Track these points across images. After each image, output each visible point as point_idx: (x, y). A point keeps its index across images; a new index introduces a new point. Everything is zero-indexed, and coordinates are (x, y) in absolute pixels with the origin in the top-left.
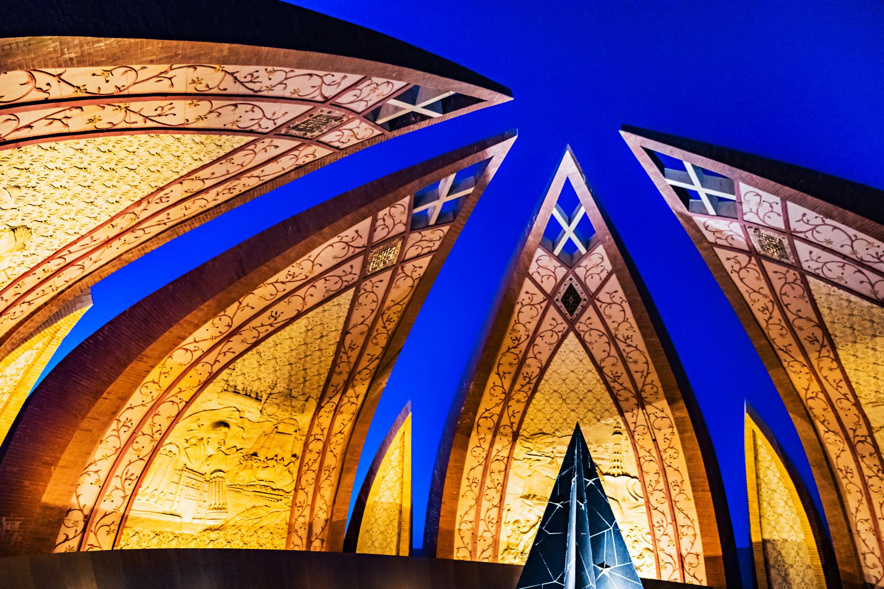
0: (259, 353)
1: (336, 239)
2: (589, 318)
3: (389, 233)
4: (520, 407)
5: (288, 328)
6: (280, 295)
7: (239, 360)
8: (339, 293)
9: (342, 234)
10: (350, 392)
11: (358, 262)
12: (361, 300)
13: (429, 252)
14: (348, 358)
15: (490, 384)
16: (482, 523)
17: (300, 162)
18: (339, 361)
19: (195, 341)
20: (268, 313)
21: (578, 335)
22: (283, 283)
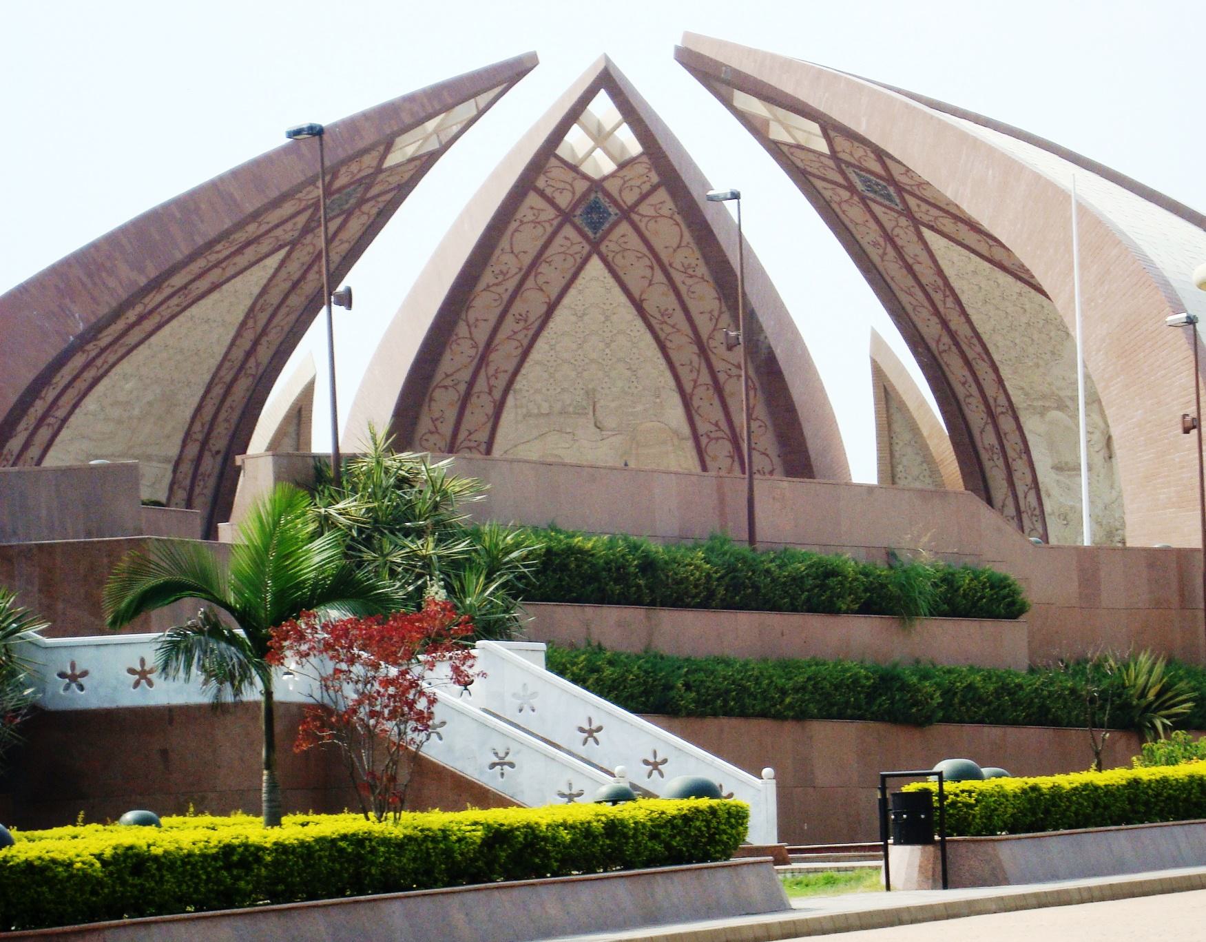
0: (537, 363)
1: (514, 225)
2: (919, 206)
3: (574, 193)
4: (969, 333)
5: (551, 324)
6: (506, 297)
7: (519, 378)
8: (580, 268)
9: (519, 215)
10: (719, 365)
11: (568, 231)
12: (619, 261)
13: (654, 188)
14: (673, 327)
15: (909, 308)
16: (1024, 516)
17: (374, 211)
18: (662, 336)
19: (447, 376)
20: (509, 319)
21: (932, 228)
22: (497, 285)
